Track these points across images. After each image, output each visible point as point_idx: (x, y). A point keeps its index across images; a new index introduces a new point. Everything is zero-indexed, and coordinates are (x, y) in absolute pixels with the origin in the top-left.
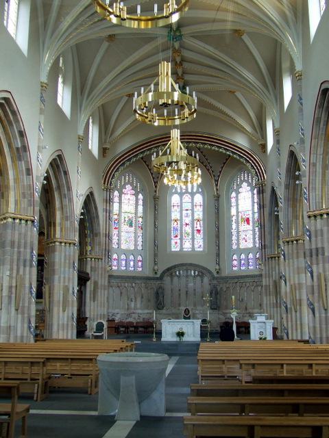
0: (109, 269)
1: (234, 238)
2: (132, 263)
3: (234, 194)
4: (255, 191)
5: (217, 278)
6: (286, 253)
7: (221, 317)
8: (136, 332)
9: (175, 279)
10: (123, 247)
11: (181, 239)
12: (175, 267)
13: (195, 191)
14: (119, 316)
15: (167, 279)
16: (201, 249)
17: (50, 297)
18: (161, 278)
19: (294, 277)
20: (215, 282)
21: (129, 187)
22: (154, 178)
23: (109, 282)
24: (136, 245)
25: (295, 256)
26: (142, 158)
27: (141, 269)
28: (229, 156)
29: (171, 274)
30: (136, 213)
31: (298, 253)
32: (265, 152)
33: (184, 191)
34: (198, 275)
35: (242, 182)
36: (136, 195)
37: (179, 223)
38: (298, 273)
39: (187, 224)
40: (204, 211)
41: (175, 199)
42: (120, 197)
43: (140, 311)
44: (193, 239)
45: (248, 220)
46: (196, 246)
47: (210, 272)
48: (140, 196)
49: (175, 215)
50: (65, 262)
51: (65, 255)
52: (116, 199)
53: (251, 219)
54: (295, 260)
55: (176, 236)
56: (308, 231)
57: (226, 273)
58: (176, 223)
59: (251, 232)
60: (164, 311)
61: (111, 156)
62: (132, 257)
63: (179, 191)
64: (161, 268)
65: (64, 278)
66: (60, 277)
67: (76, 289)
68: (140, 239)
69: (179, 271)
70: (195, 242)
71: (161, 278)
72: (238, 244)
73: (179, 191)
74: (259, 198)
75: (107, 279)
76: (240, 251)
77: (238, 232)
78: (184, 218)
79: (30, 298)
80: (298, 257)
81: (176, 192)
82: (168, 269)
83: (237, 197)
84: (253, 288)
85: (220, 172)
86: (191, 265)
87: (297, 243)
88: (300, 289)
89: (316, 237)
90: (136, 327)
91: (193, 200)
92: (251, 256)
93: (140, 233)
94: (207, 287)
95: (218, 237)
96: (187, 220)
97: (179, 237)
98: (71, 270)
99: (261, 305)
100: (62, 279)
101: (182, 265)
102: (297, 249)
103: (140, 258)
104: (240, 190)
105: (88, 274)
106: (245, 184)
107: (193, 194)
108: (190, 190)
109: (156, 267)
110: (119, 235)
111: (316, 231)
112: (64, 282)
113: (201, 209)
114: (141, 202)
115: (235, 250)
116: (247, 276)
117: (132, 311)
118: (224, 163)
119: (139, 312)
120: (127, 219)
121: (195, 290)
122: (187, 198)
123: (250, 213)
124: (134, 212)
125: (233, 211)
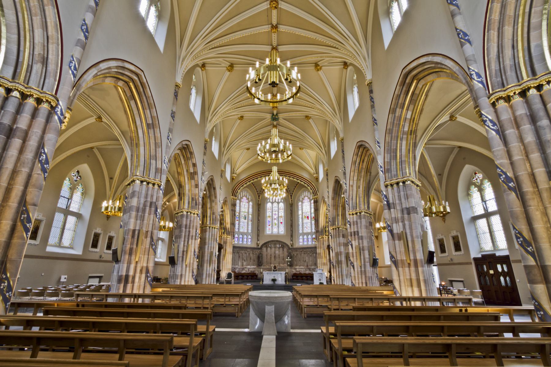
0: (233, 243)
1: (300, 227)
2: (245, 240)
3: (300, 203)
4: (312, 201)
6: (332, 234)
7: (293, 270)
8: (247, 279)
9: (269, 249)
10: (241, 230)
11: (272, 227)
13: (280, 201)
14: (237, 269)
15: (264, 249)
16: (283, 233)
17: (202, 258)
18: (261, 248)
19: (337, 248)
21: (244, 198)
23: (233, 250)
24: (248, 230)
25: (337, 236)
26: (252, 183)
28: (298, 183)
30: (248, 212)
31: (339, 235)
32: (317, 181)
36: (248, 202)
38: (340, 246)
40: (284, 212)
41: (269, 205)
42: (240, 203)
44: (278, 227)
45: (308, 217)
46: (280, 231)
47: (287, 245)
48: (251, 203)
49: (269, 213)
50: (212, 238)
51: (212, 234)
52: (238, 205)
54: (338, 239)
56: (349, 222)
57: (296, 246)
59: (310, 224)
61: (235, 182)
62: (245, 236)
63: (271, 201)
64: (261, 243)
65: (211, 247)
66: (208, 247)
67: (217, 253)
68: (250, 227)
70: (280, 229)
71: (261, 248)
72: (303, 230)
73: (271, 201)
74: (315, 205)
76: (303, 234)
77: (303, 224)
78: (274, 216)
79: (194, 258)
80: (339, 237)
81: (270, 202)
83: (302, 205)
84: (311, 254)
86: (277, 241)
87: (339, 229)
88: (341, 255)
89: (354, 225)
90: (248, 276)
91: (278, 206)
92: (310, 237)
93: (250, 223)
94: (286, 254)
95: (292, 226)
96: (275, 217)
97: (271, 226)
98: (215, 242)
99: (315, 264)
100: (210, 248)
101: (272, 241)
102: (339, 233)
103: (250, 237)
104: (304, 201)
105: (222, 245)
106: (306, 198)
107: (278, 203)
108: (277, 201)
109: (258, 242)
110: (239, 224)
111: (354, 222)
112: (211, 249)
113: (283, 211)
114: (251, 207)
116: (308, 248)
117: (245, 267)
119: (250, 268)
120: (243, 216)
122: (275, 205)
123: (309, 213)
124: (247, 211)
125: (300, 212)
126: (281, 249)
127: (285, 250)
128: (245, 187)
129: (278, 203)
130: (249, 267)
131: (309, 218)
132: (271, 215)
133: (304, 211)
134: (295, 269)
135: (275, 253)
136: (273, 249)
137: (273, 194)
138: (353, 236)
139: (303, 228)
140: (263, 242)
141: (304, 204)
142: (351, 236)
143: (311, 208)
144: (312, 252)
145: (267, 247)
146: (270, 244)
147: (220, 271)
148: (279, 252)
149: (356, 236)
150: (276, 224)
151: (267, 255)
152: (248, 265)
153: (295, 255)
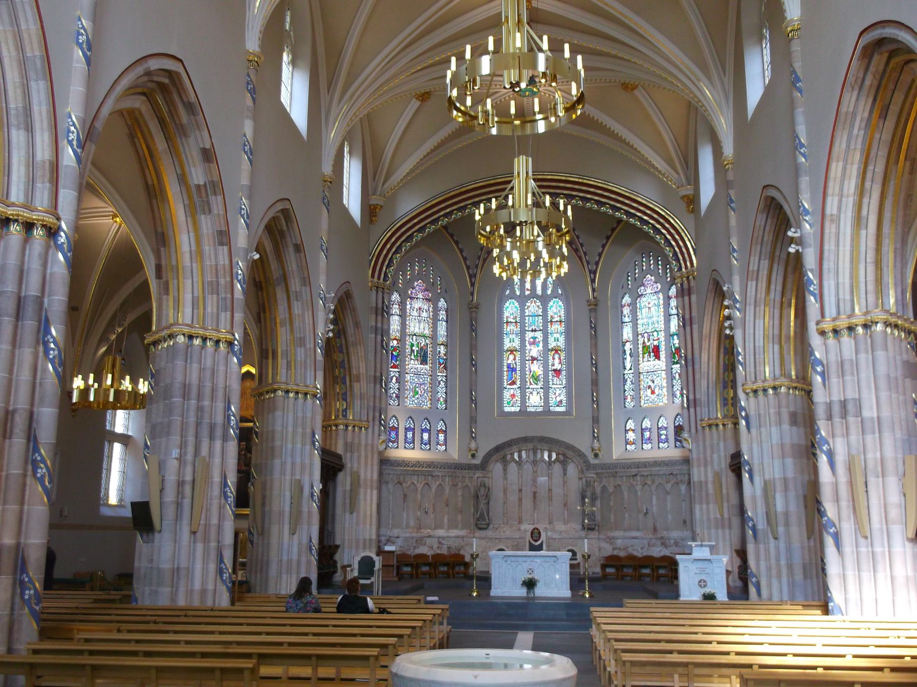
0: (382, 447)
4: (673, 291)
5: (595, 466)
7: (604, 545)
9: (512, 467)
11: (523, 388)
12: (509, 444)
13: (549, 292)
15: (497, 468)
16: (562, 409)
18: (483, 466)
20: (591, 475)
22: (468, 268)
23: (381, 474)
24: (434, 400)
26: (445, 227)
27: (444, 448)
28: (620, 221)
29: (504, 457)
30: (434, 337)
33: (527, 293)
34: (557, 460)
35: (643, 274)
36: (432, 301)
37: (518, 354)
39: (533, 359)
41: (511, 309)
42: (402, 305)
43: (441, 532)
44: (546, 389)
45: (656, 351)
46: (553, 401)
47: (581, 455)
48: (442, 303)
52: (395, 309)
53: (662, 348)
55: (513, 383)
58: (511, 357)
59: (664, 375)
60: (489, 533)
68: (441, 389)
69: (520, 452)
70: (551, 395)
71: (483, 466)
72: (637, 398)
75: (376, 468)
76: (641, 413)
77: (638, 374)
81: (513, 296)
82: (498, 449)
84: (668, 487)
85: (600, 255)
86: (543, 440)
91: (545, 311)
93: (441, 375)
96: (534, 351)
97: (518, 383)
101: (525, 440)
105: (339, 457)
107: (544, 300)
108: (539, 291)
113: (561, 328)
114: (442, 315)
115: (631, 411)
118: (608, 238)
121: (550, 490)
122: (533, 307)
125: (627, 333)
126: (557, 468)
127: (572, 469)
128: (418, 244)
129: (544, 300)
130: (441, 532)
131: (663, 355)
132: (516, 344)
133: (640, 329)
134: (611, 540)
135: (534, 481)
136: (528, 467)
137: (522, 264)
138: (837, 420)
139: (637, 389)
140: (493, 446)
141: (643, 302)
142: (830, 418)
143: (668, 316)
144: (673, 480)
145: (505, 462)
146: (515, 448)
147: (337, 547)
148: (550, 477)
149: (851, 419)
150: (536, 379)
151: (505, 491)
152: (437, 527)
153: (611, 489)
